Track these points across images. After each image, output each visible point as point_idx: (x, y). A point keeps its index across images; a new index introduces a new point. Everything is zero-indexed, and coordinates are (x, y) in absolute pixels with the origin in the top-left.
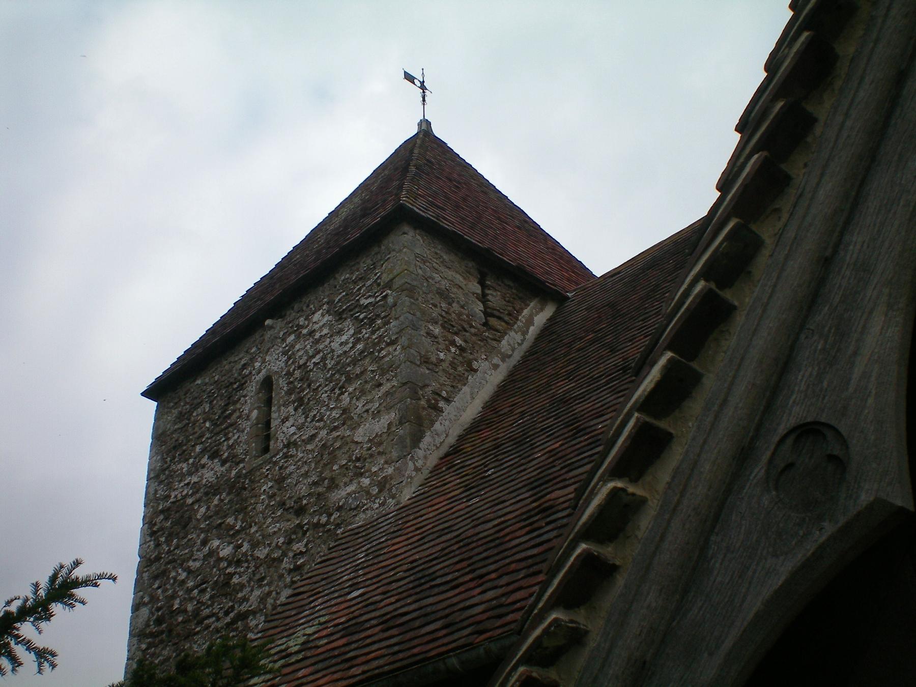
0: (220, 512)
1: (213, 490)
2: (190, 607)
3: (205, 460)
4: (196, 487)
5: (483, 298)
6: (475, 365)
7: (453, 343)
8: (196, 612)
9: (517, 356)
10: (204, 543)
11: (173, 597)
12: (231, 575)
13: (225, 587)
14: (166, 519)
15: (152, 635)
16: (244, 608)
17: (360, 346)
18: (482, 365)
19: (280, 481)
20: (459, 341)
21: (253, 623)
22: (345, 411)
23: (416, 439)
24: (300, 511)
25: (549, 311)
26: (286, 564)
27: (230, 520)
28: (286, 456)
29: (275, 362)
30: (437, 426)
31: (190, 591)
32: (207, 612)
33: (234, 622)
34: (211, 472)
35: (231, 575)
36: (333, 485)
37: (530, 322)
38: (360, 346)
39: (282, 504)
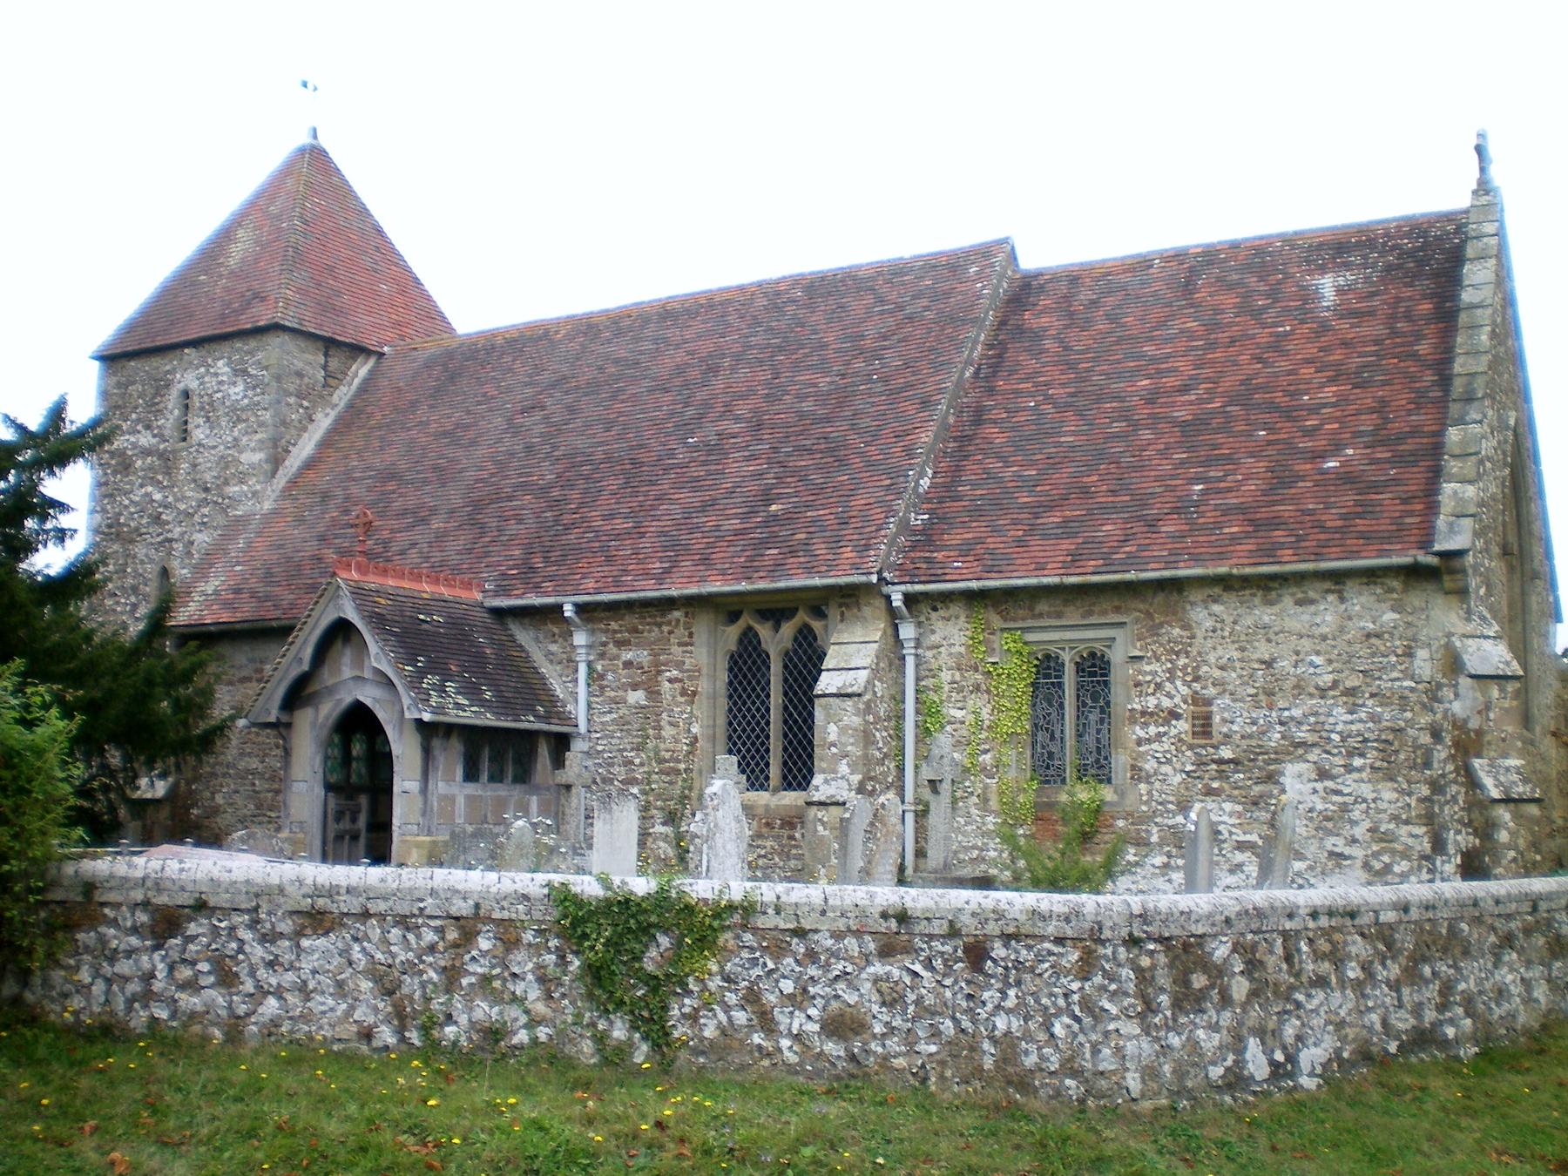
0: (151, 468)
1: (147, 452)
2: (132, 524)
3: (139, 427)
4: (135, 446)
5: (325, 367)
6: (314, 417)
7: (301, 406)
8: (137, 529)
9: (342, 404)
10: (142, 486)
11: (120, 514)
12: (161, 513)
13: (157, 519)
14: (112, 458)
15: (103, 533)
16: (170, 535)
17: (246, 401)
18: (319, 416)
19: (194, 466)
20: (306, 403)
21: (175, 546)
22: (235, 439)
23: (274, 473)
24: (207, 490)
25: (371, 362)
26: (197, 518)
27: (160, 477)
28: (197, 451)
29: (189, 380)
30: (287, 463)
31: (132, 514)
32: (144, 530)
33: (163, 542)
34: (146, 439)
35: (161, 513)
36: (226, 483)
37: (356, 375)
38: (246, 401)
39: (195, 481)
